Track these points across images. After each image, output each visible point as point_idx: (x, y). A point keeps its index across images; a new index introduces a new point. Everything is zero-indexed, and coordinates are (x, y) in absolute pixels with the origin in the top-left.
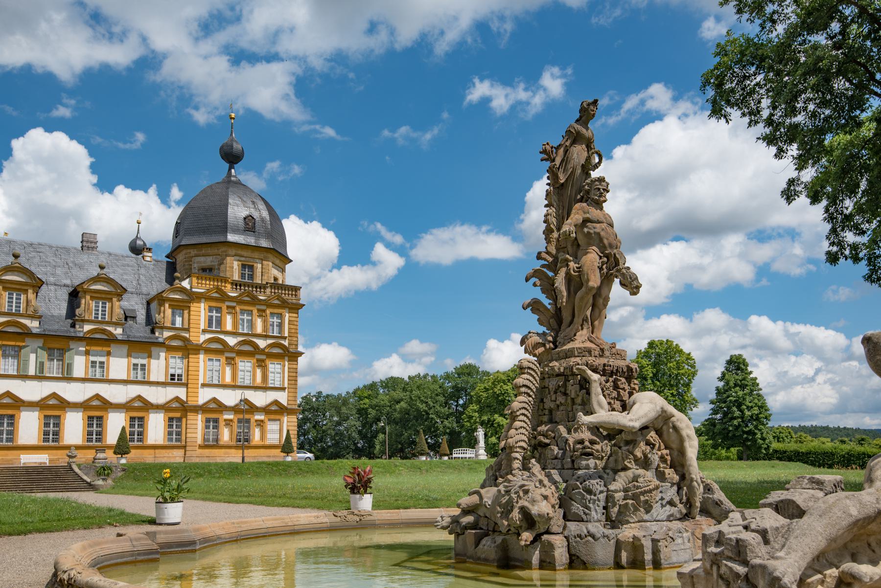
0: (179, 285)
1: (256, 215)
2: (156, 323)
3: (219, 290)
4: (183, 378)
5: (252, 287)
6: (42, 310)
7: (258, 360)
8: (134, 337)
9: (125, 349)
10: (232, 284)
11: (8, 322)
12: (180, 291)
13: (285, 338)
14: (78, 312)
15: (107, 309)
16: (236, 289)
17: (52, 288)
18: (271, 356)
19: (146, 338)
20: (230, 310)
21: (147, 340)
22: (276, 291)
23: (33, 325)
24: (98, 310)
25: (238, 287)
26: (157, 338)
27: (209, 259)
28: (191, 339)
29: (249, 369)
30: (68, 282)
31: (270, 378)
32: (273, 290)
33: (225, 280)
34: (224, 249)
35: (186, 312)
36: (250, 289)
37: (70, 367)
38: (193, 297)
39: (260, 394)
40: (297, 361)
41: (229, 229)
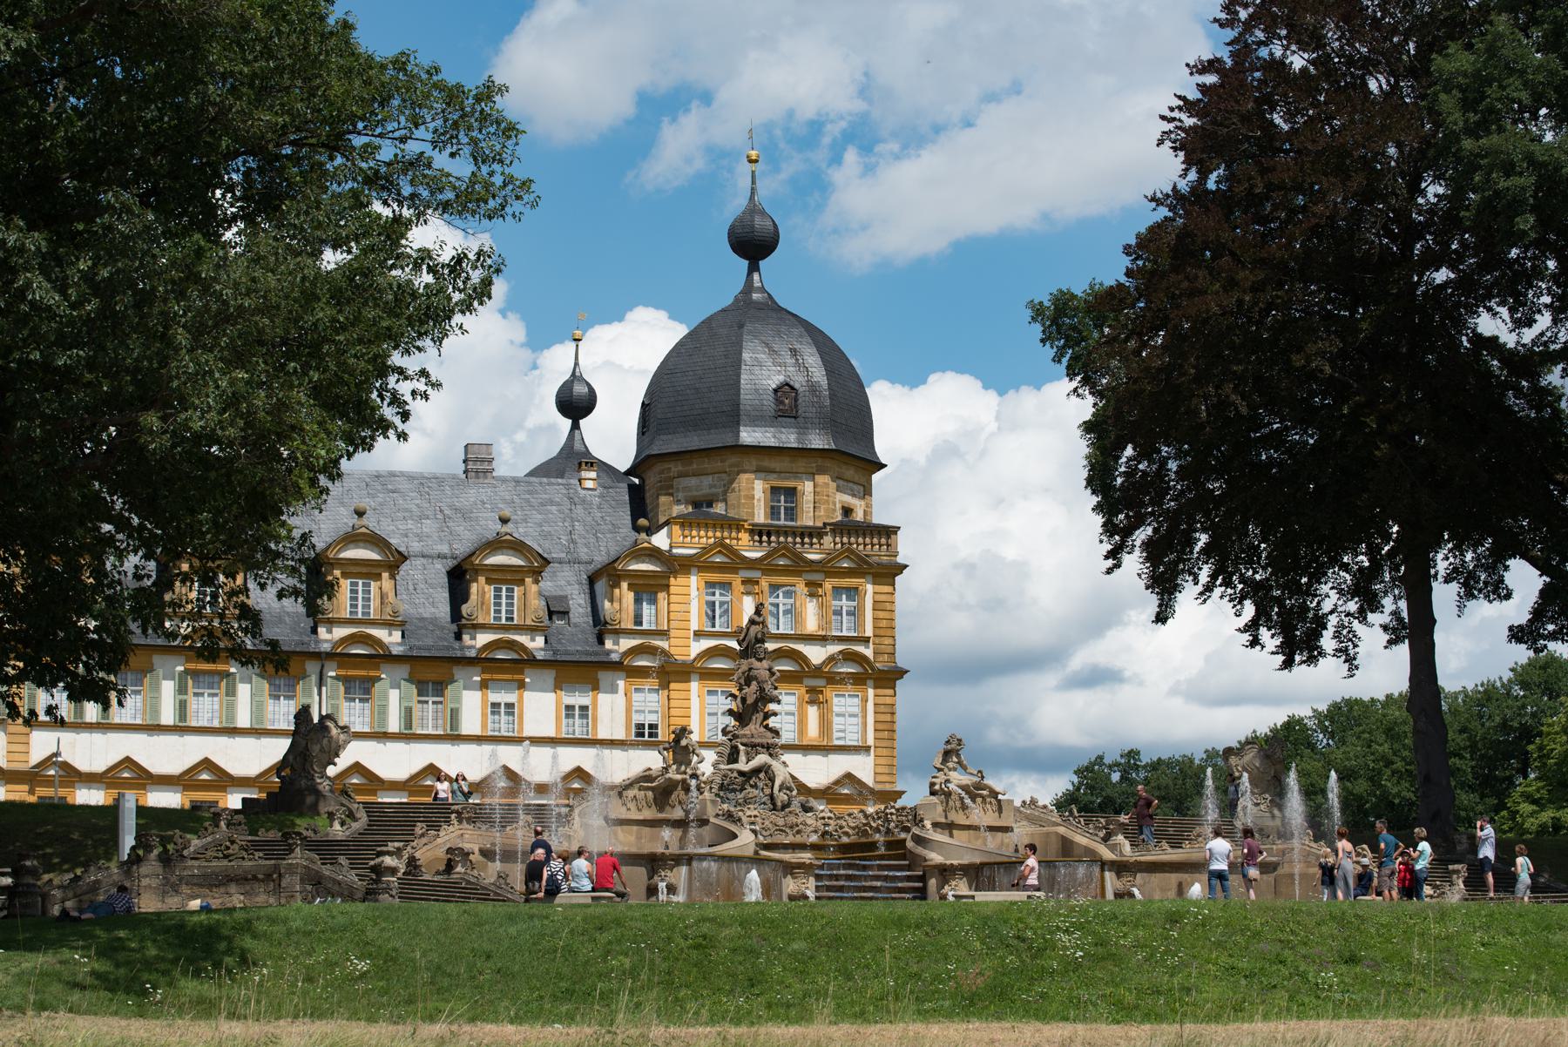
0: (646, 545)
1: (798, 381)
2: (606, 623)
3: (722, 547)
4: (659, 731)
5: (794, 535)
6: (405, 608)
7: (812, 691)
8: (567, 653)
9: (549, 676)
10: (752, 532)
11: (352, 636)
12: (650, 555)
13: (866, 640)
14: (465, 609)
15: (515, 601)
16: (761, 542)
17: (419, 562)
18: (833, 679)
19: (587, 653)
20: (749, 587)
21: (589, 659)
22: (845, 540)
23: (391, 639)
24: (498, 604)
25: (765, 538)
26: (611, 651)
27: (707, 480)
28: (673, 651)
29: (793, 708)
30: (444, 549)
31: (835, 727)
32: (838, 539)
33: (734, 524)
34: (733, 459)
35: (661, 596)
36: (790, 539)
37: (455, 715)
38: (675, 565)
39: (815, 760)
40: (894, 688)
41: (743, 417)
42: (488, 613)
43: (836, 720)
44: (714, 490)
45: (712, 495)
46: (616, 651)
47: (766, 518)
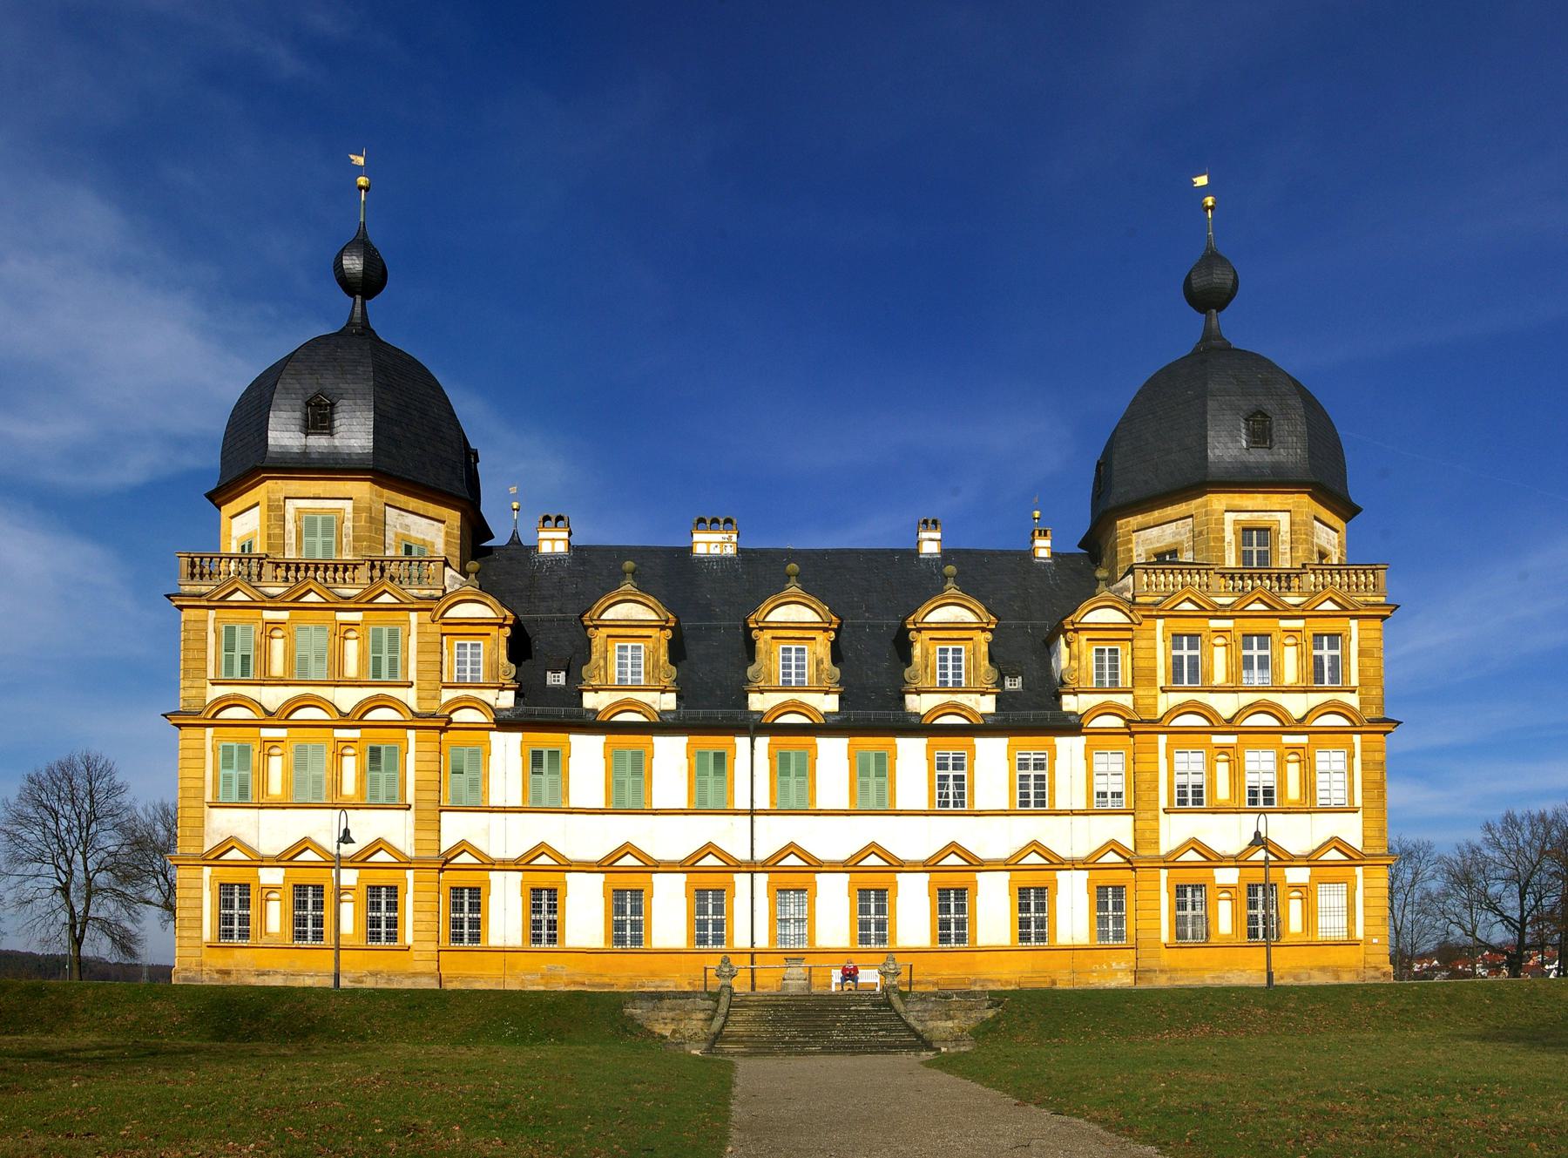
11: (784, 705)
24: (946, 667)
27: (1169, 529)
31: (1319, 786)
42: (933, 677)
43: (1320, 777)
44: (1178, 538)
45: (1176, 543)
46: (1074, 713)
47: (1237, 563)
